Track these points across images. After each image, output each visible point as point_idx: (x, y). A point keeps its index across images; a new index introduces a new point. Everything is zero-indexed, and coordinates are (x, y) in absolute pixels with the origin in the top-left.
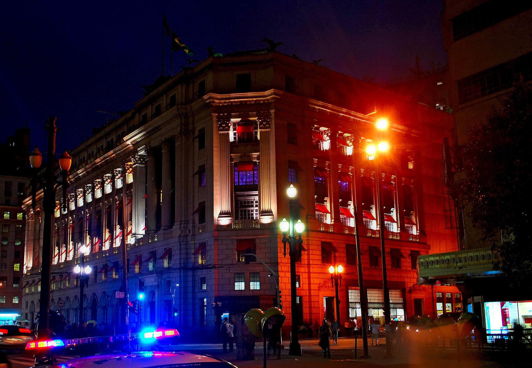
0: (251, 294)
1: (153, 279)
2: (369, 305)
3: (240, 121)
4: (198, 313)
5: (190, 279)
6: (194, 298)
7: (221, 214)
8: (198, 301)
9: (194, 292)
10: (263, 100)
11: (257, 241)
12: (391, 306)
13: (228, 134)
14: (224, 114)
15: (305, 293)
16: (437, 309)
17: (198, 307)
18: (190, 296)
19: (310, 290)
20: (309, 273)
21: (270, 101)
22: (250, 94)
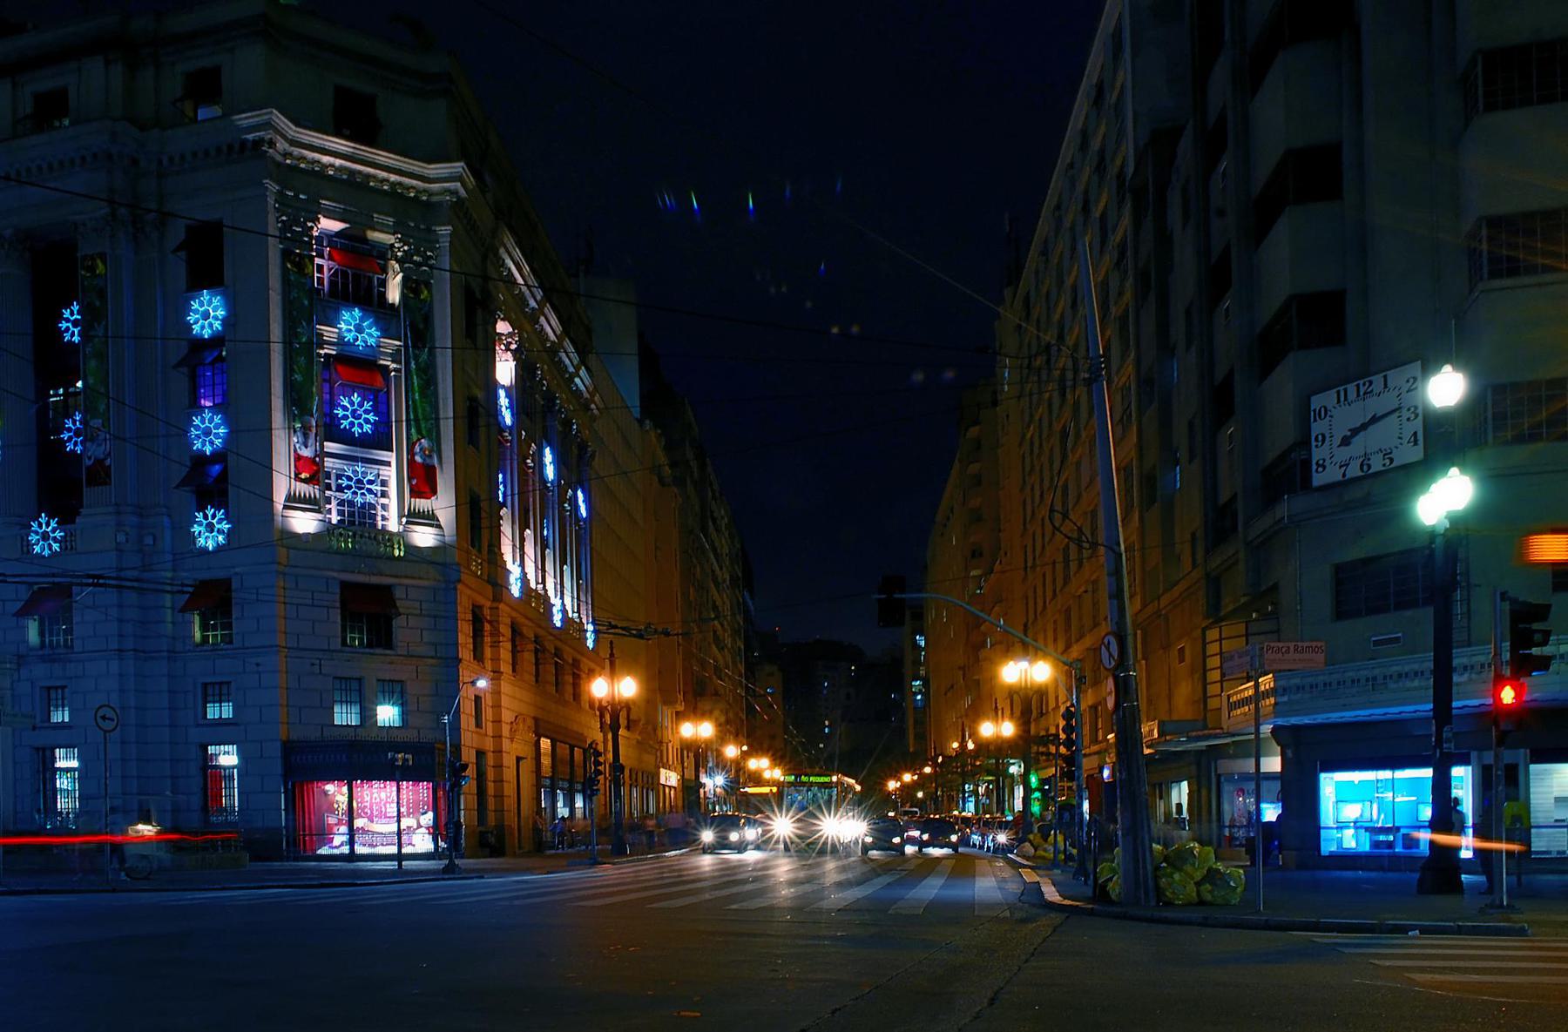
3: (339, 234)
10: (418, 191)
11: (399, 593)
14: (296, 196)
21: (435, 199)
22: (383, 157)
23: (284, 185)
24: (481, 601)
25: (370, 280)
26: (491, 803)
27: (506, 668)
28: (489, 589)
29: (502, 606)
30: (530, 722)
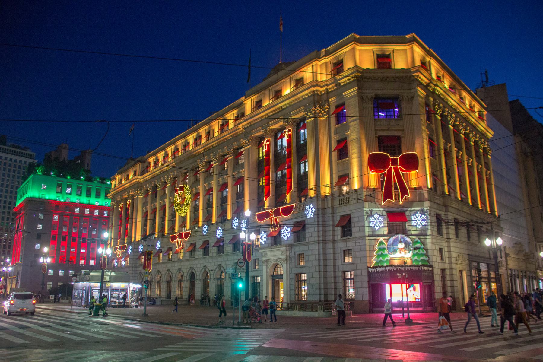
1: (280, 253)
4: (340, 286)
6: (335, 271)
8: (340, 274)
9: (335, 265)
15: (447, 266)
17: (341, 280)
19: (450, 263)
20: (449, 246)
24: (440, 212)
26: (449, 283)
27: (452, 236)
28: (444, 208)
29: (449, 213)
30: (466, 256)
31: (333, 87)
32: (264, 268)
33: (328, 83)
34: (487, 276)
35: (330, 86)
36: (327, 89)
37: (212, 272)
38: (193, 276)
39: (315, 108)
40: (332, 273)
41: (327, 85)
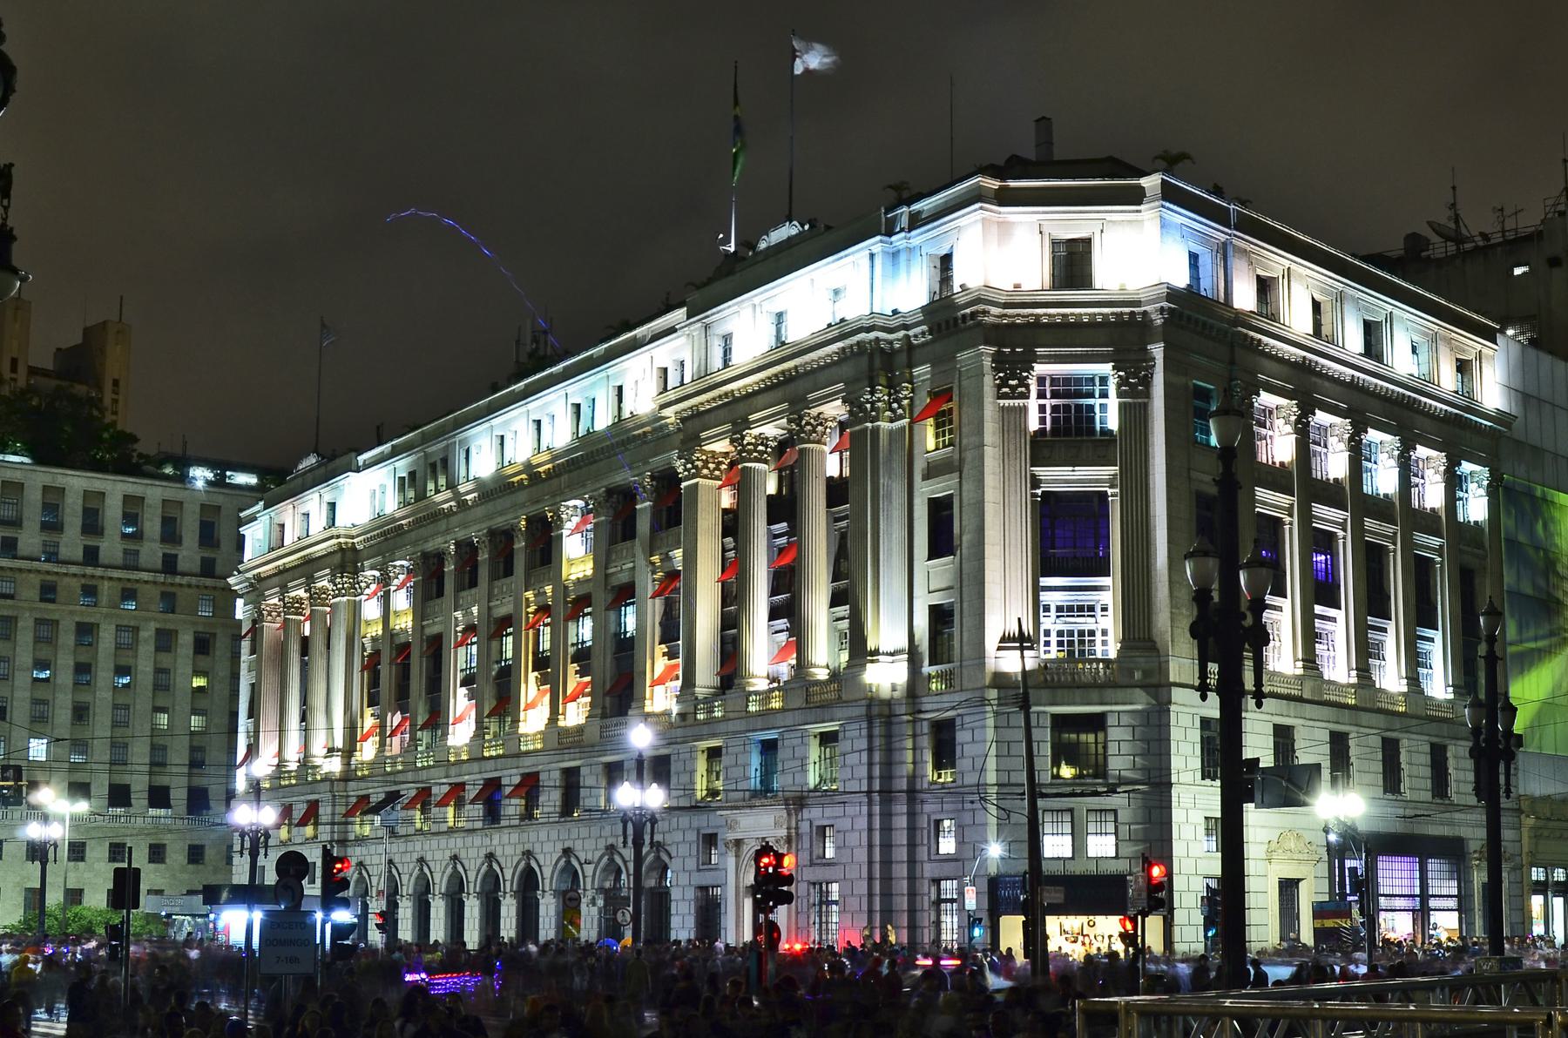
0: (1092, 869)
2: (1383, 901)
5: (901, 822)
6: (912, 878)
7: (1003, 640)
9: (912, 861)
12: (1433, 903)
13: (1025, 409)
14: (1013, 351)
16: (1456, 914)
18: (901, 871)
23: (1000, 345)
25: (1091, 408)
31: (923, 333)
32: (731, 861)
33: (909, 321)
34: (1417, 891)
35: (918, 330)
36: (908, 337)
37: (589, 869)
38: (529, 882)
39: (872, 393)
40: (905, 883)
41: (906, 327)
